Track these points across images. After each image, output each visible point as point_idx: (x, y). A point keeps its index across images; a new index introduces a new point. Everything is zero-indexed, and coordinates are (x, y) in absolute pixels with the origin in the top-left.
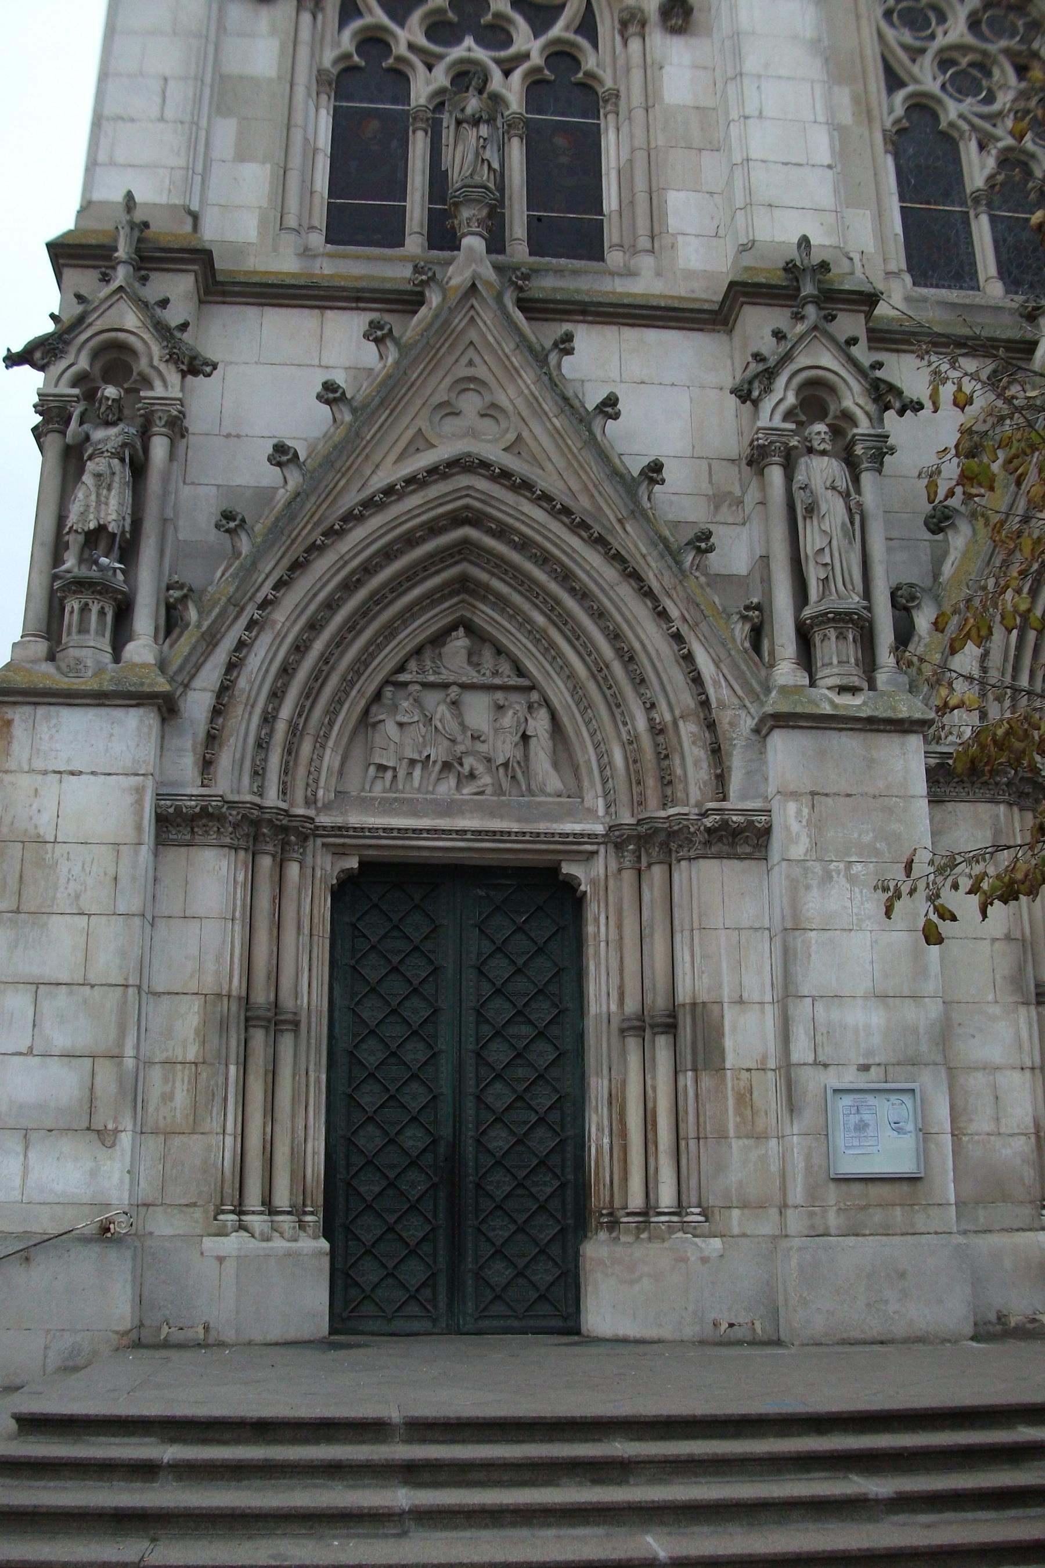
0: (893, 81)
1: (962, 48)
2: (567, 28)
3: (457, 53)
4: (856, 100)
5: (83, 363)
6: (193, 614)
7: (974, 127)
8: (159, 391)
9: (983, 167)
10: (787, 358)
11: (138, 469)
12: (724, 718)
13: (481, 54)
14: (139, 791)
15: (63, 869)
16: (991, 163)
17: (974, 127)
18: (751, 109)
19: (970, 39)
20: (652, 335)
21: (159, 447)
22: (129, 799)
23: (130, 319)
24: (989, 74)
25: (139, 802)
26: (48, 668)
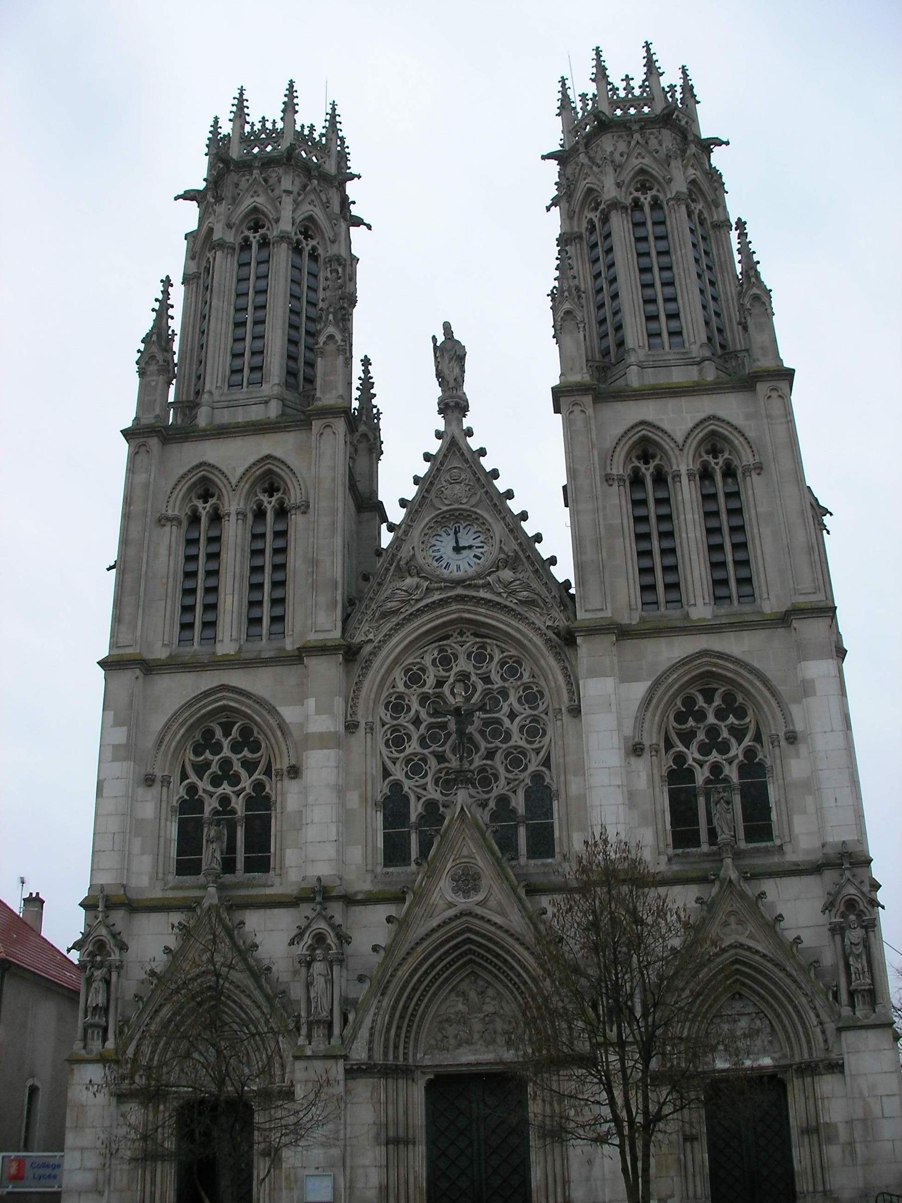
0: (386, 773)
1: (416, 754)
3: (220, 791)
4: (360, 796)
5: (91, 948)
6: (126, 1030)
7: (415, 792)
8: (113, 957)
9: (416, 810)
10: (308, 926)
11: (108, 982)
12: (285, 1055)
16: (420, 809)
17: (415, 792)
18: (309, 821)
19: (419, 750)
20: (277, 911)
21: (114, 976)
23: (104, 931)
24: (426, 763)
26: (83, 1052)
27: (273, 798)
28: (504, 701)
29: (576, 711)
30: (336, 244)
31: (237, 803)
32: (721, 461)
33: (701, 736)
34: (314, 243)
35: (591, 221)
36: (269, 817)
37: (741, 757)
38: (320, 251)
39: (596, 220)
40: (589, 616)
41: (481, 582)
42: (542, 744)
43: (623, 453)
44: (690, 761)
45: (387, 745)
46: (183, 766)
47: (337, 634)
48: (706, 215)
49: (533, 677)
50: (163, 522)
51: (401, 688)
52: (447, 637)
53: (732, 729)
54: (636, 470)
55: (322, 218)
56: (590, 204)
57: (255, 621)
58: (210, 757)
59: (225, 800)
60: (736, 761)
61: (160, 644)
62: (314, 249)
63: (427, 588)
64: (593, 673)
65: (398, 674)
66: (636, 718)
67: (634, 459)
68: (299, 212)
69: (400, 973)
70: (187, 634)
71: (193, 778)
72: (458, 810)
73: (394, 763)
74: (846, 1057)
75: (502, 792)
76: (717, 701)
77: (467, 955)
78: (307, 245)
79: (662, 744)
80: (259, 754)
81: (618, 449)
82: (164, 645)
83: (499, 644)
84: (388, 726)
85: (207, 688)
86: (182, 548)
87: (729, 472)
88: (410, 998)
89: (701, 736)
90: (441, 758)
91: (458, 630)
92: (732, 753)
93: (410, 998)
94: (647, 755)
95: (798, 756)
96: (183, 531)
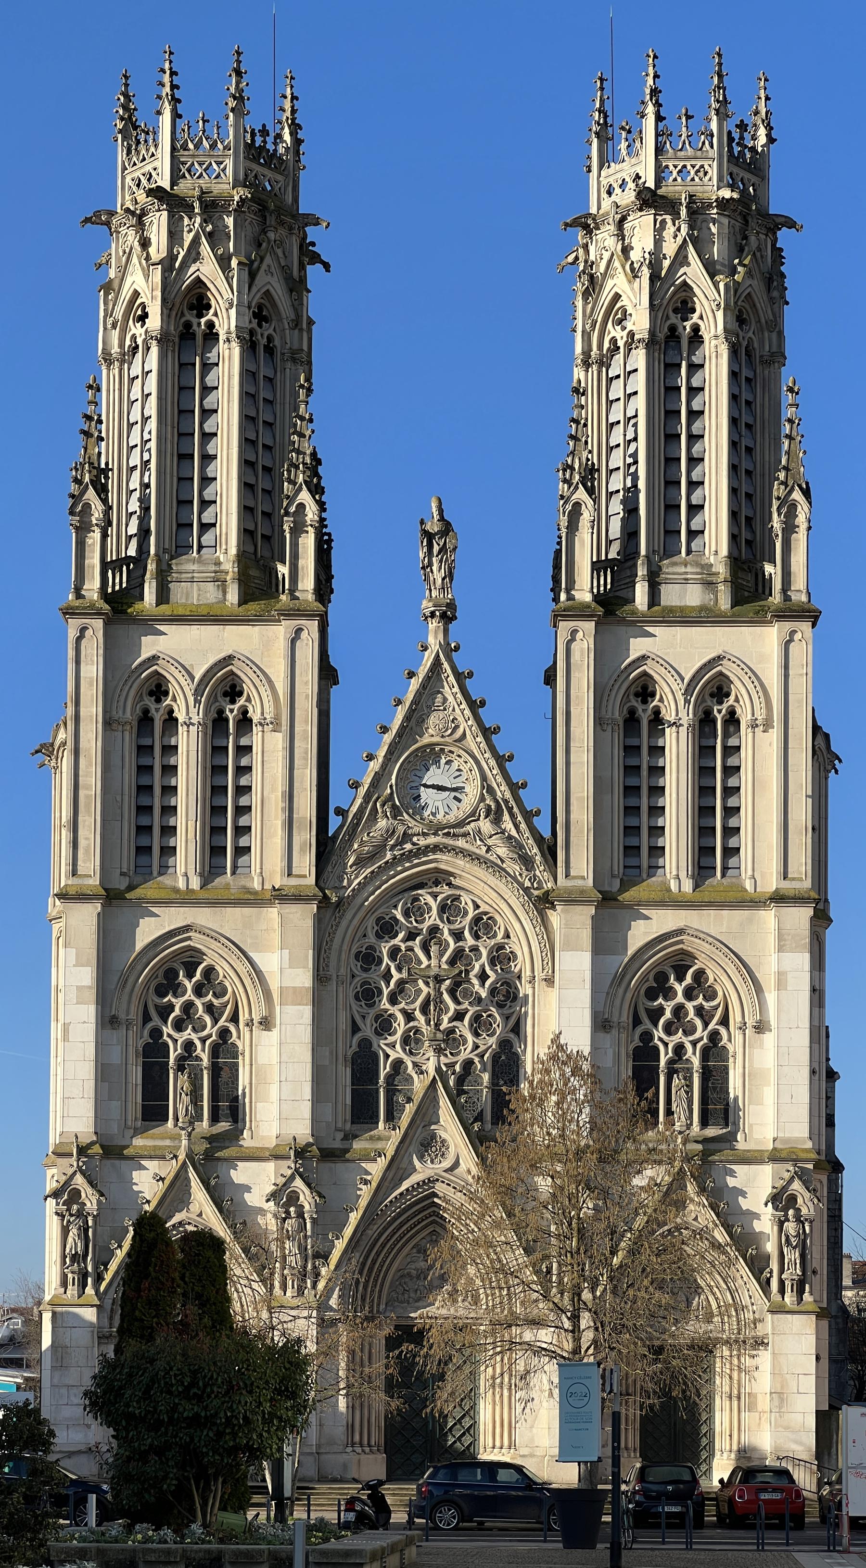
0: (355, 1029)
2: (226, 1021)
4: (331, 1053)
13: (194, 1037)
14: (93, 1332)
15: (73, 1355)
22: (90, 1334)
25: (93, 1335)
27: (241, 1048)
28: (476, 961)
29: (549, 981)
30: (296, 331)
31: (204, 1050)
32: (724, 707)
33: (668, 1014)
34: (271, 331)
35: (614, 341)
36: (236, 1065)
37: (705, 1040)
38: (277, 342)
39: (621, 343)
40: (570, 883)
41: (462, 830)
42: (512, 1011)
43: (622, 691)
44: (656, 1041)
45: (357, 998)
46: (146, 1006)
47: (312, 880)
48: (756, 345)
49: (508, 937)
50: (115, 726)
51: (372, 939)
52: (421, 886)
53: (699, 1011)
54: (632, 712)
55: (280, 292)
56: (616, 314)
57: (218, 851)
58: (173, 1000)
59: (189, 1046)
60: (702, 1043)
61: (118, 871)
62: (270, 339)
63: (405, 833)
64: (568, 946)
65: (371, 922)
66: (608, 993)
67: (631, 697)
68: (254, 289)
69: (370, 1232)
70: (143, 860)
71: (156, 1021)
72: (431, 1078)
73: (364, 1017)
74: (770, 1336)
75: (471, 1056)
76: (689, 979)
77: (431, 1216)
78: (262, 335)
79: (631, 1019)
80: (226, 998)
81: (616, 687)
82: (123, 874)
83: (476, 899)
84: (357, 979)
85: (172, 927)
86: (134, 755)
87: (732, 720)
88: (378, 1254)
89: (668, 1014)
90: (409, 1017)
91: (434, 879)
92: (697, 1035)
93: (378, 1254)
94: (614, 1032)
95: (761, 1046)
96: (134, 736)
